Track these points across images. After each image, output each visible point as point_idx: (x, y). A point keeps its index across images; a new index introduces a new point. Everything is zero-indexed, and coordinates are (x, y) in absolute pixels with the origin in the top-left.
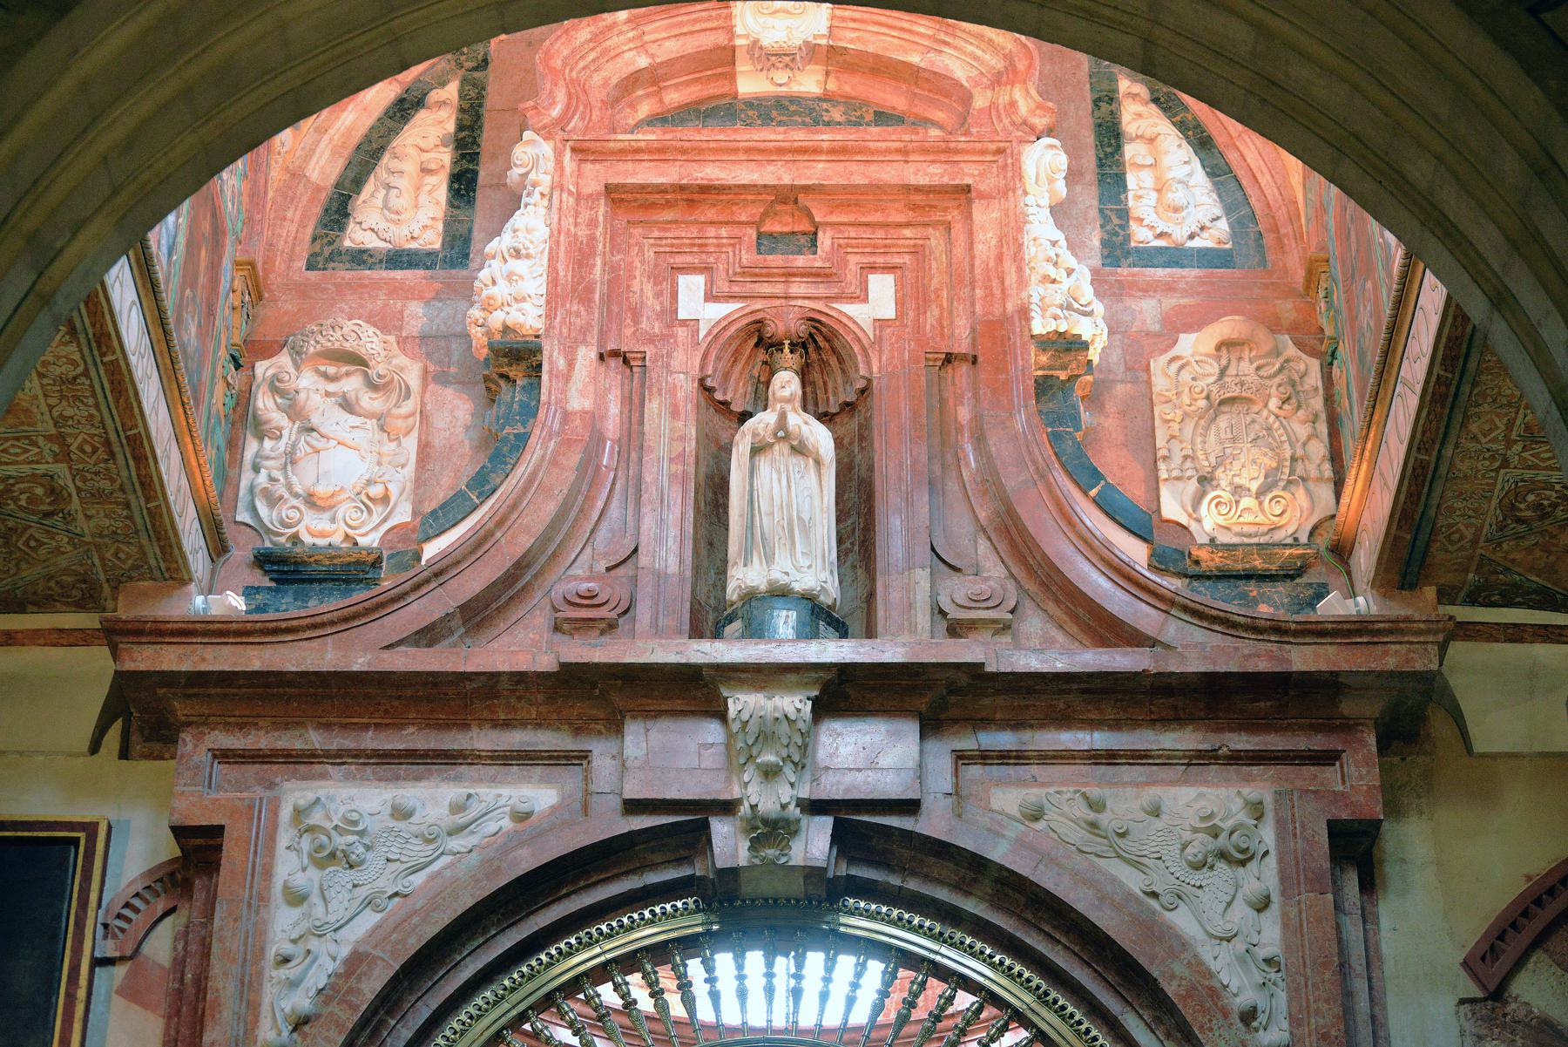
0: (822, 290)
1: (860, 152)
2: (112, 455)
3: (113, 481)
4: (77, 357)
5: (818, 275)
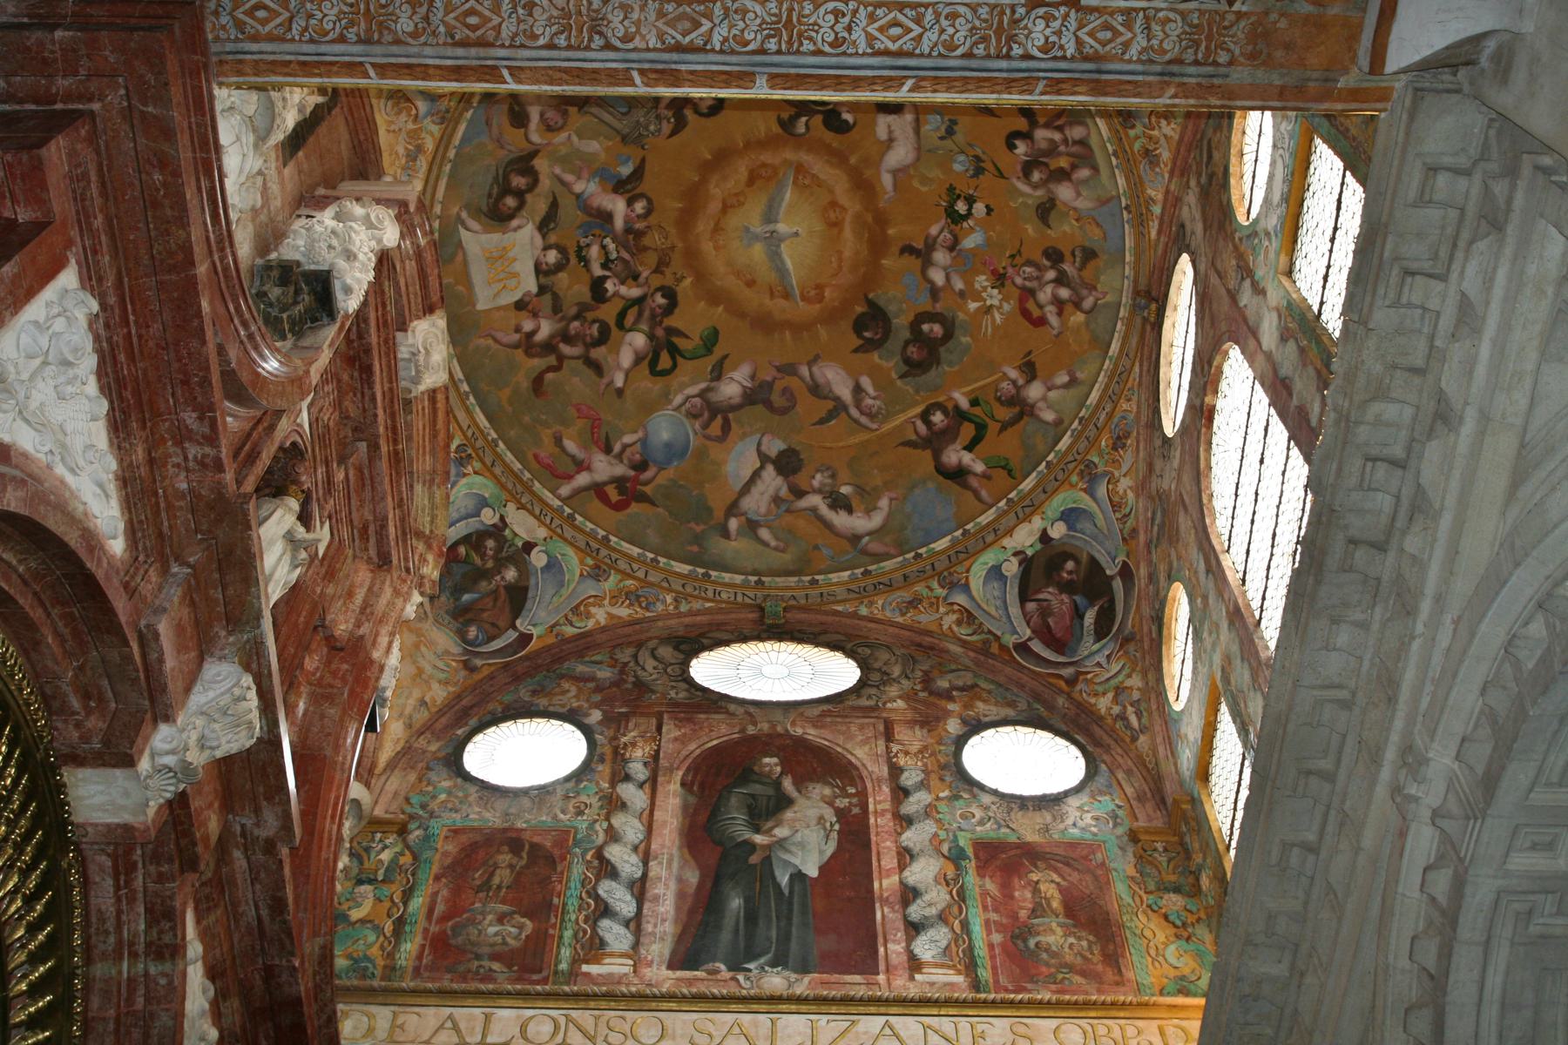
0: (321, 492)
1: (397, 473)
2: (464, 44)
3: (415, 35)
4: (637, 42)
5: (329, 484)
